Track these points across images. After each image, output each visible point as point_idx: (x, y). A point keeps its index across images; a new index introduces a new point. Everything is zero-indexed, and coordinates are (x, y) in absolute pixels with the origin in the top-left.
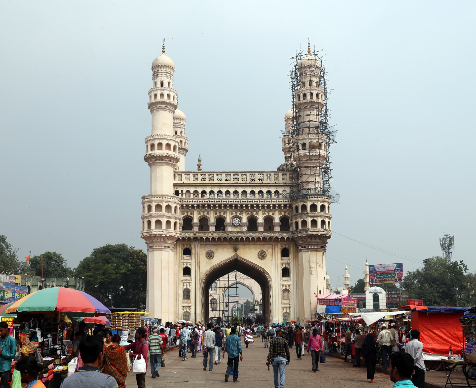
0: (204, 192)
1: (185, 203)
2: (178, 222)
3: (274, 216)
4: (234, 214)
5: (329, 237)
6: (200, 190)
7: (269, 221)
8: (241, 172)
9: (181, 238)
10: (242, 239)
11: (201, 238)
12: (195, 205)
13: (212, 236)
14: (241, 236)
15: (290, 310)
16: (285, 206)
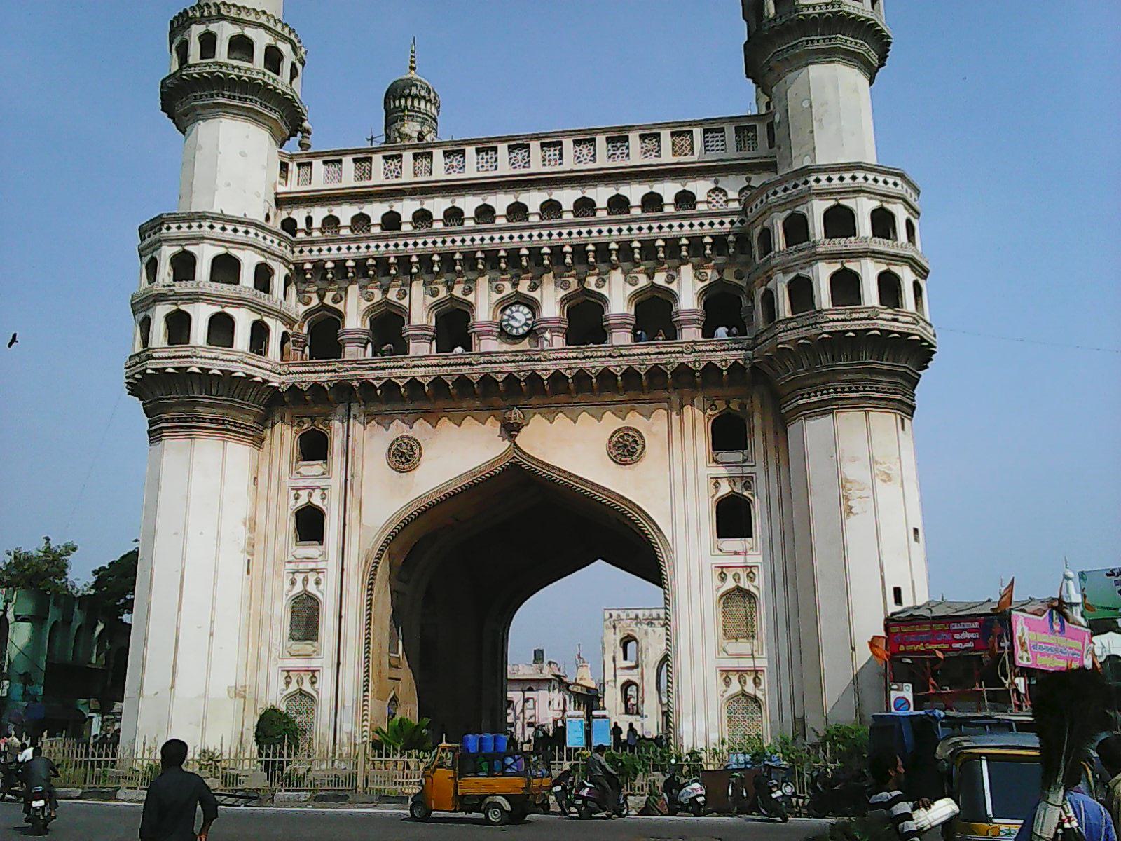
0: (391, 221)
1: (308, 256)
2: (276, 329)
3: (673, 286)
4: (508, 289)
5: (921, 352)
6: (376, 211)
7: (654, 314)
8: (537, 137)
9: (284, 388)
10: (534, 378)
11: (366, 385)
12: (350, 263)
13: (408, 373)
14: (529, 366)
15: (756, 682)
16: (719, 241)
